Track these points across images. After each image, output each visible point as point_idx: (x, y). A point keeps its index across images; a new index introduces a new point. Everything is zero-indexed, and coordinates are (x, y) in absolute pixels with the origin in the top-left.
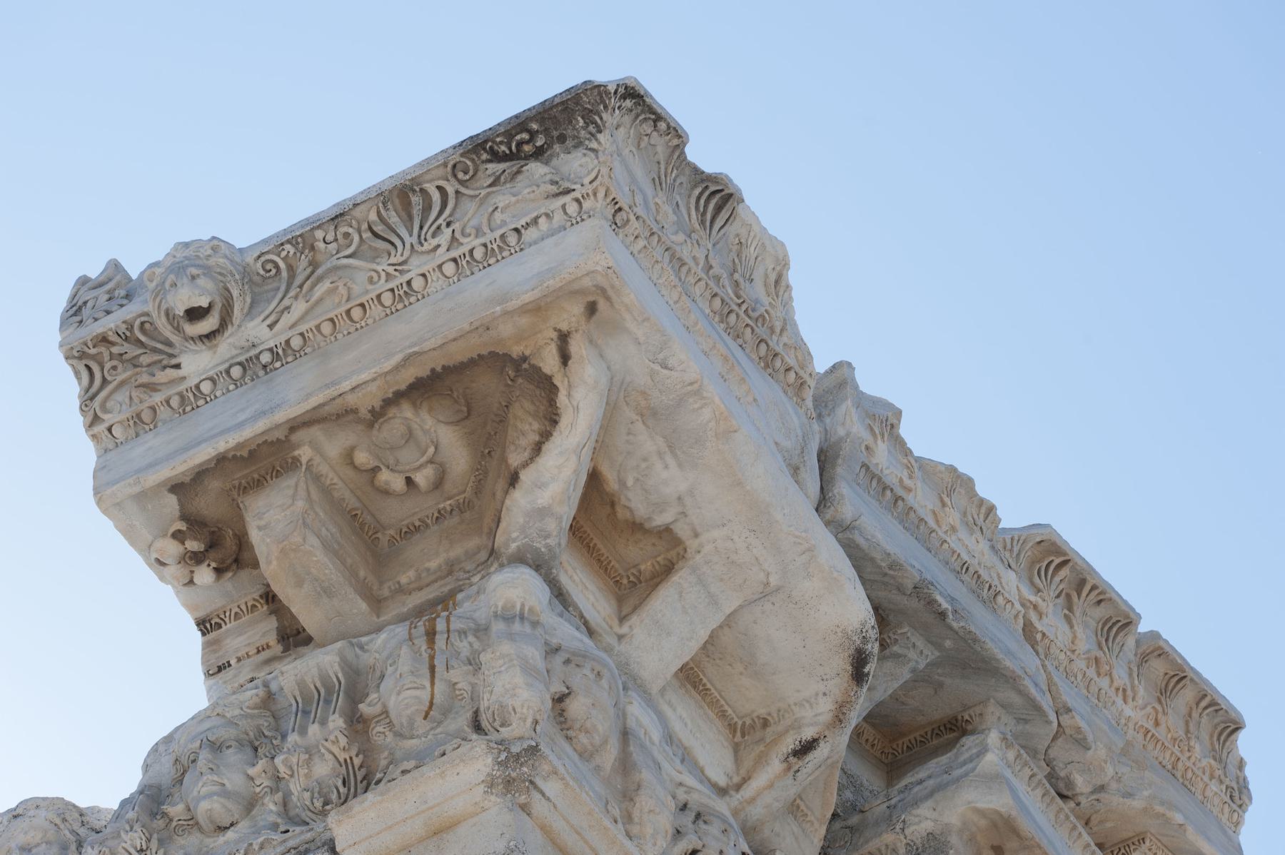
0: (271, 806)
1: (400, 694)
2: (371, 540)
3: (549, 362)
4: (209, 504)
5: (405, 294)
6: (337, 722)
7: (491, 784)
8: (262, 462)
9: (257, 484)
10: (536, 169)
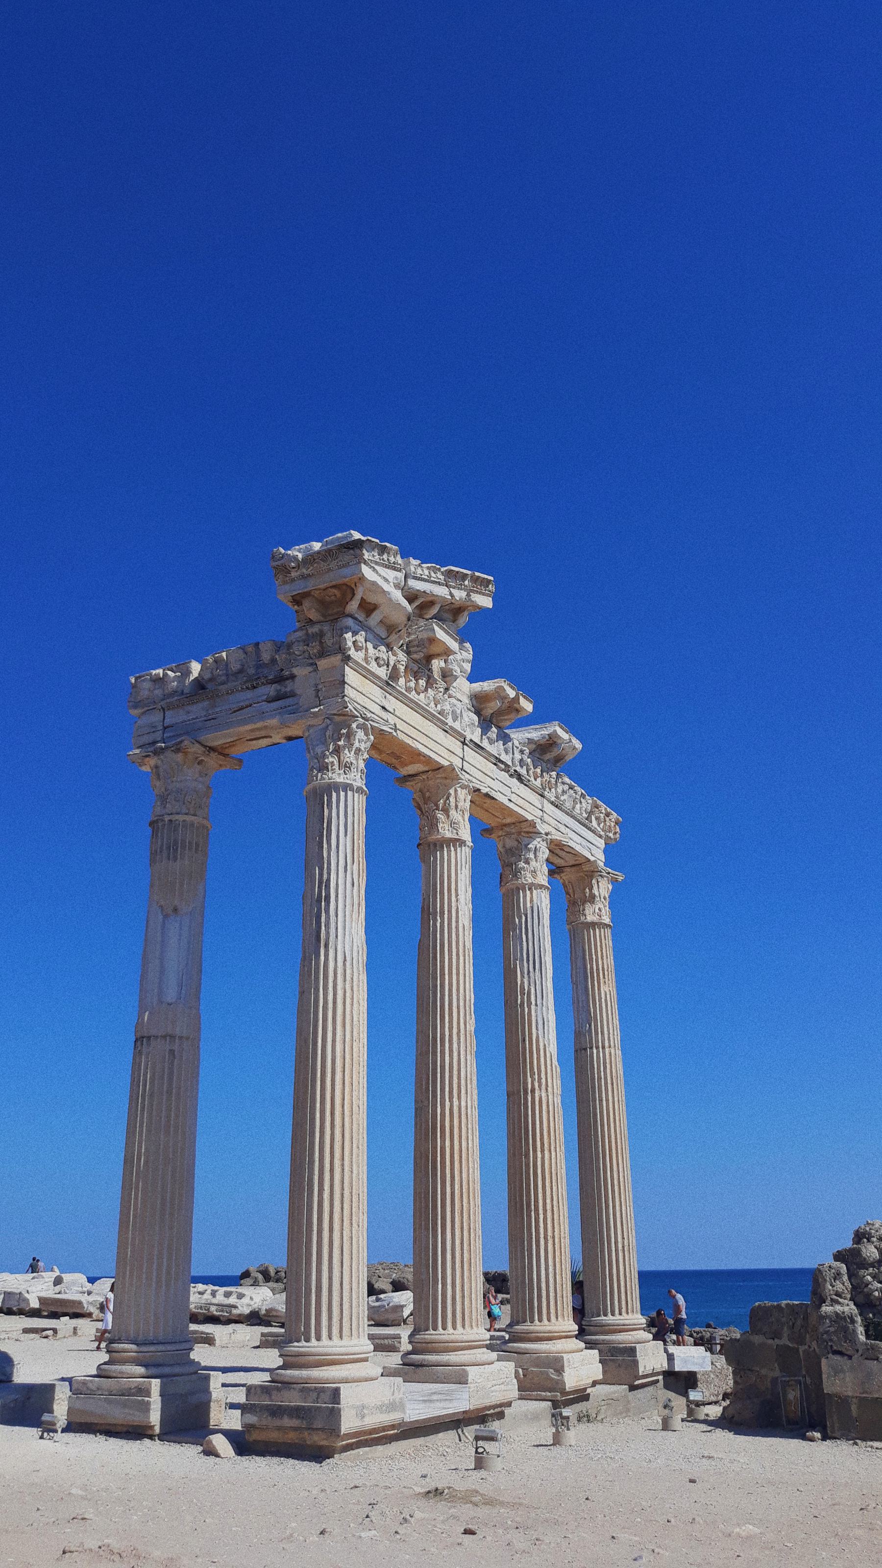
0: (306, 655)
1: (329, 641)
2: (323, 605)
3: (353, 586)
4: (298, 598)
5: (330, 570)
6: (317, 643)
7: (342, 660)
8: (306, 595)
9: (303, 598)
10: (352, 551)
